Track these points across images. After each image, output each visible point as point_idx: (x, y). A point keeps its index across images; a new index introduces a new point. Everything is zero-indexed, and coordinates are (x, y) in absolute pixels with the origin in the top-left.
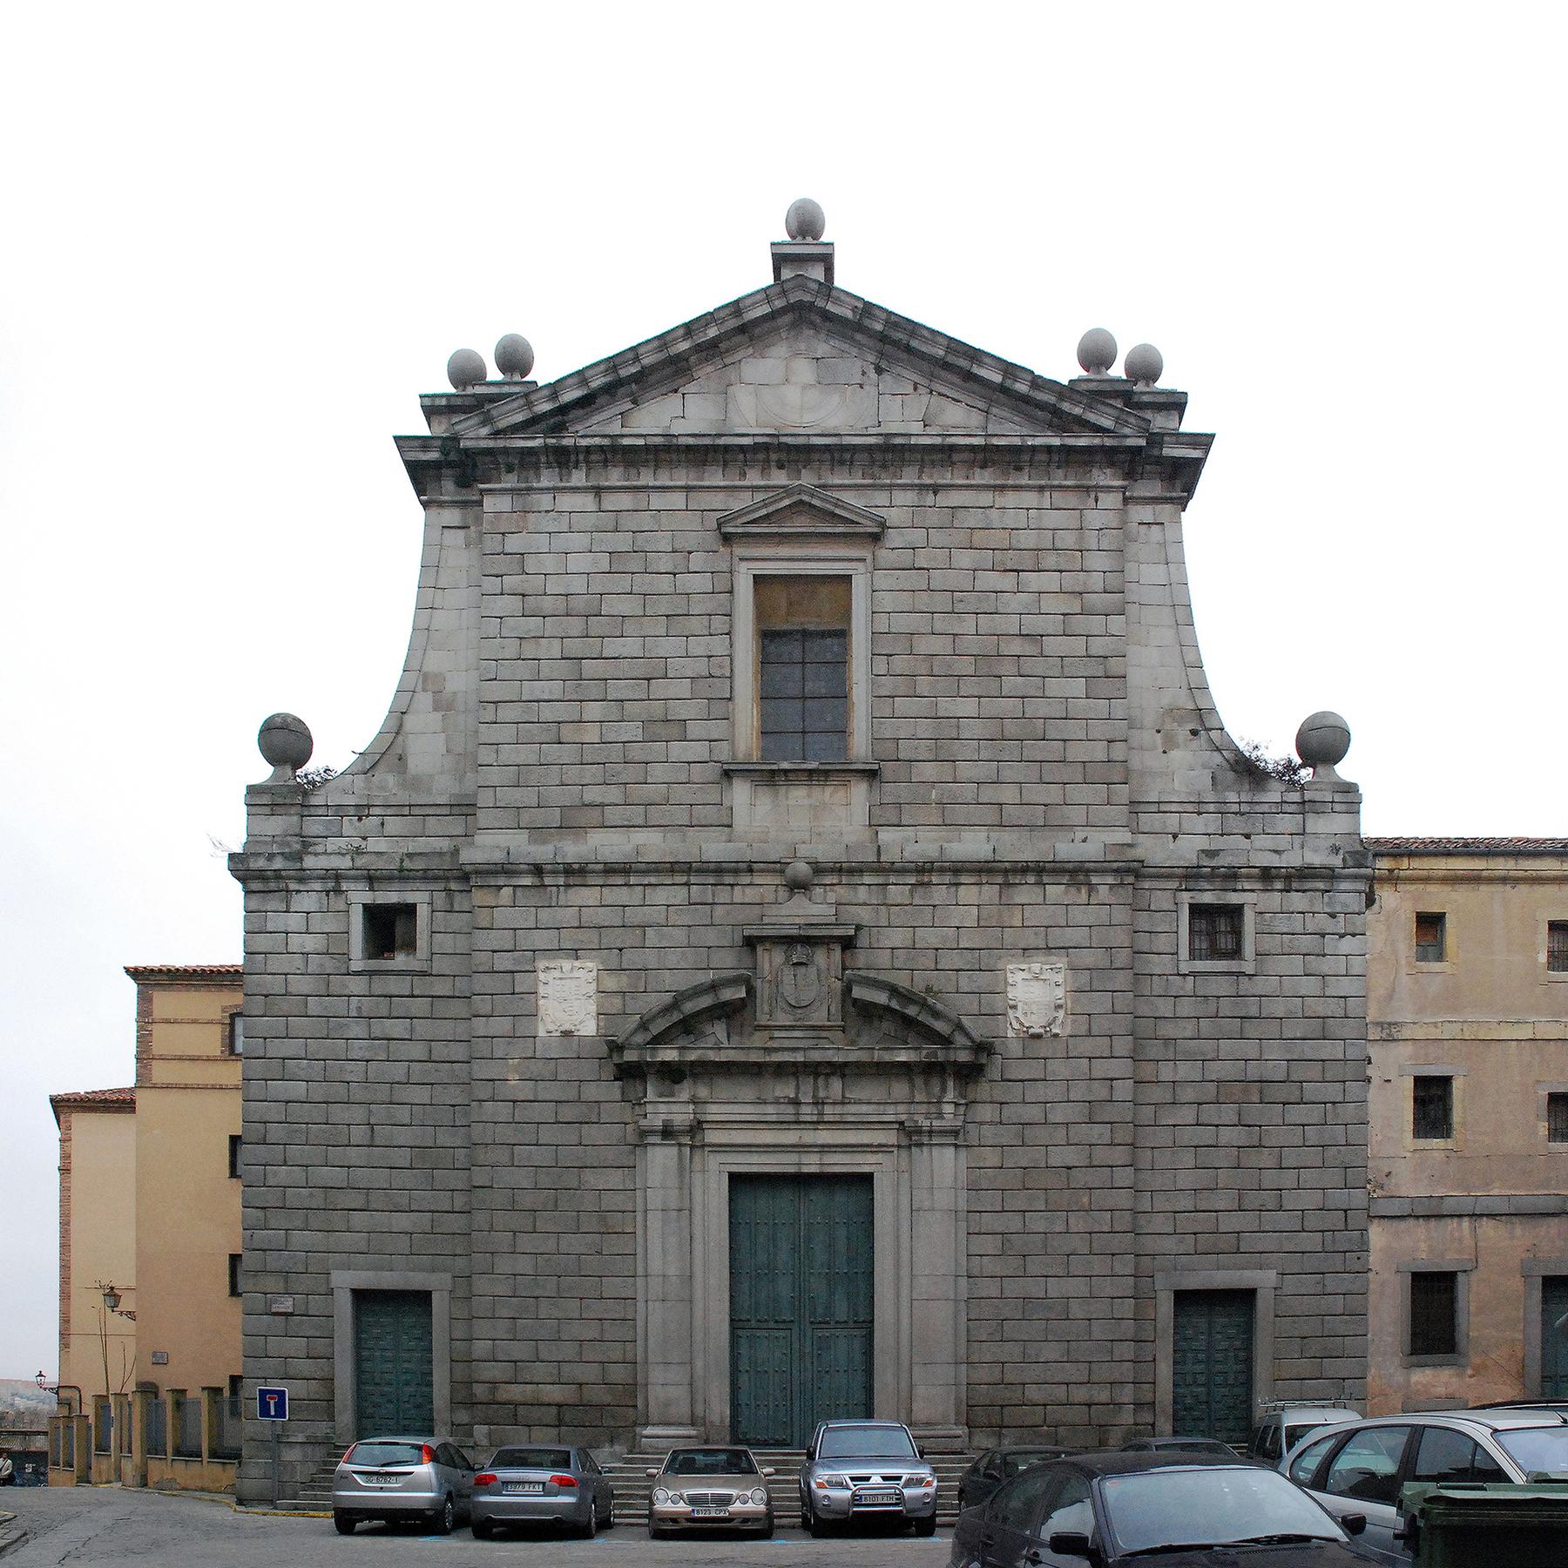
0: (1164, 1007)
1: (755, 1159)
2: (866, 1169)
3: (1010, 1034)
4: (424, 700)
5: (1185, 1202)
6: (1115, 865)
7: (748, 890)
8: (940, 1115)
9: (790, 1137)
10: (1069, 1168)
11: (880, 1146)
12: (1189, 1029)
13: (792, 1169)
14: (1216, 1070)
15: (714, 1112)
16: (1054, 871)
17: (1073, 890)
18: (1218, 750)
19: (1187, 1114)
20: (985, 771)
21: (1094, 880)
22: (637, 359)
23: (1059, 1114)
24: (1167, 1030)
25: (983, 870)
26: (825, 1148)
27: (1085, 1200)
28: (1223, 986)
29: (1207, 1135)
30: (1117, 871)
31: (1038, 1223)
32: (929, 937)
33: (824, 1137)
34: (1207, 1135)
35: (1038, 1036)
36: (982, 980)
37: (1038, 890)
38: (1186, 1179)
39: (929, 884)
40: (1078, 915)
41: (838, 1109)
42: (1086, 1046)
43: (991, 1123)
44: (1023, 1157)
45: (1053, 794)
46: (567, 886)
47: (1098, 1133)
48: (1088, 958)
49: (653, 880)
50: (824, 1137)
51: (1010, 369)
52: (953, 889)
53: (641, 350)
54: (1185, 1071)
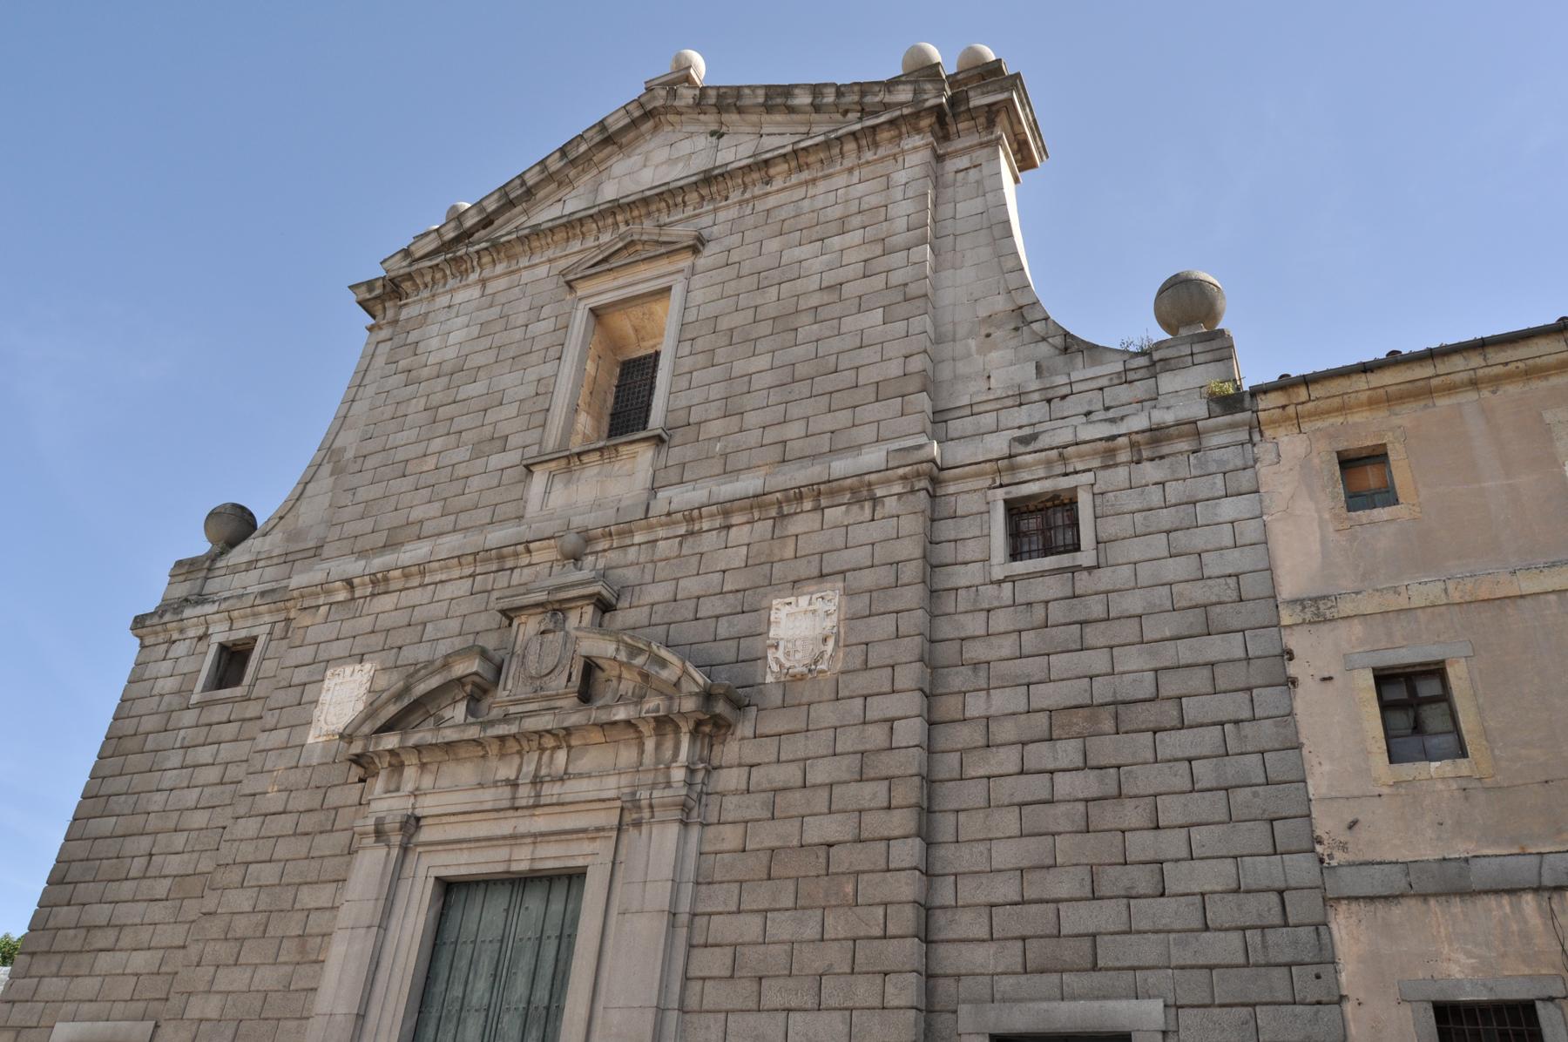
0: (974, 625)
1: (464, 857)
2: (580, 862)
3: (770, 679)
4: (326, 469)
5: (1006, 889)
6: (901, 471)
7: (526, 570)
8: (668, 785)
9: (505, 828)
10: (830, 845)
11: (598, 830)
12: (1007, 646)
13: (500, 868)
14: (1047, 696)
15: (427, 806)
16: (832, 493)
17: (855, 508)
18: (1044, 339)
19: (1006, 760)
20: (775, 413)
21: (879, 493)
22: (523, 183)
23: (820, 773)
24: (976, 651)
25: (755, 503)
26: (538, 837)
27: (849, 889)
28: (1053, 587)
29: (1036, 787)
30: (904, 478)
31: (782, 927)
32: (691, 586)
33: (541, 823)
34: (1036, 787)
35: (802, 677)
36: (742, 623)
37: (817, 516)
38: (1006, 854)
39: (701, 532)
40: (859, 534)
41: (557, 788)
42: (861, 682)
43: (735, 792)
44: (766, 836)
45: (843, 418)
46: (373, 595)
47: (873, 793)
48: (867, 579)
49: (444, 577)
50: (541, 823)
51: (816, 90)
52: (724, 533)
53: (527, 177)
54: (1003, 701)
